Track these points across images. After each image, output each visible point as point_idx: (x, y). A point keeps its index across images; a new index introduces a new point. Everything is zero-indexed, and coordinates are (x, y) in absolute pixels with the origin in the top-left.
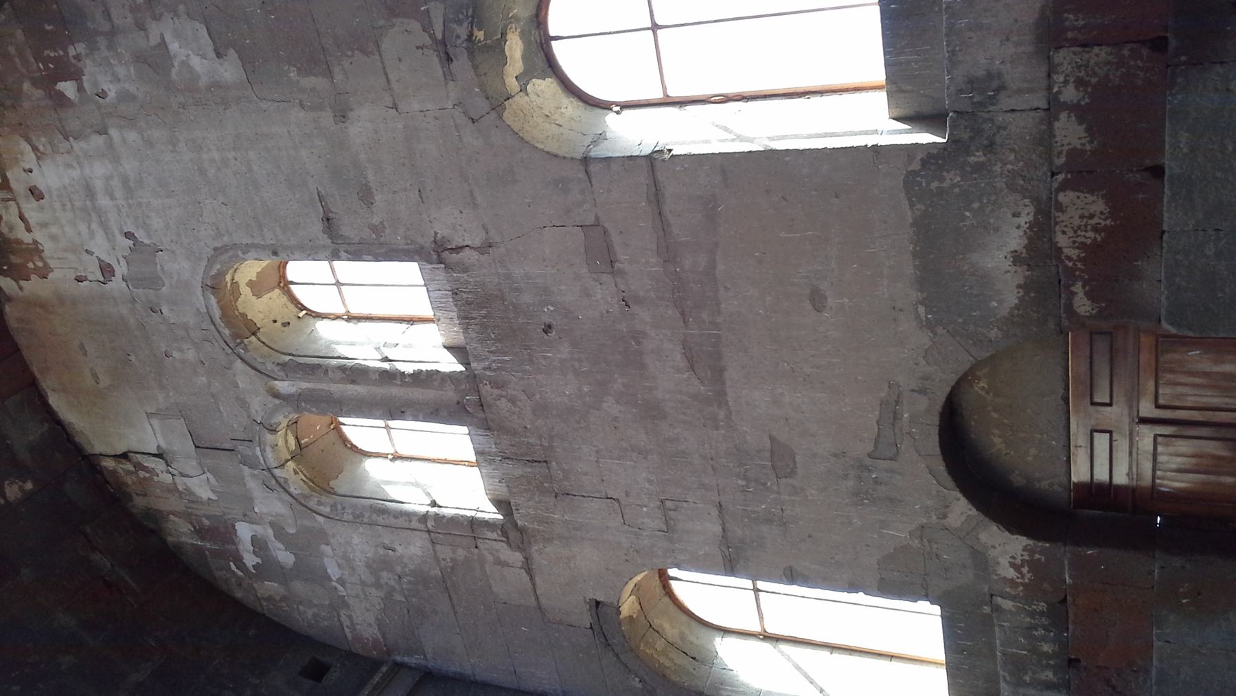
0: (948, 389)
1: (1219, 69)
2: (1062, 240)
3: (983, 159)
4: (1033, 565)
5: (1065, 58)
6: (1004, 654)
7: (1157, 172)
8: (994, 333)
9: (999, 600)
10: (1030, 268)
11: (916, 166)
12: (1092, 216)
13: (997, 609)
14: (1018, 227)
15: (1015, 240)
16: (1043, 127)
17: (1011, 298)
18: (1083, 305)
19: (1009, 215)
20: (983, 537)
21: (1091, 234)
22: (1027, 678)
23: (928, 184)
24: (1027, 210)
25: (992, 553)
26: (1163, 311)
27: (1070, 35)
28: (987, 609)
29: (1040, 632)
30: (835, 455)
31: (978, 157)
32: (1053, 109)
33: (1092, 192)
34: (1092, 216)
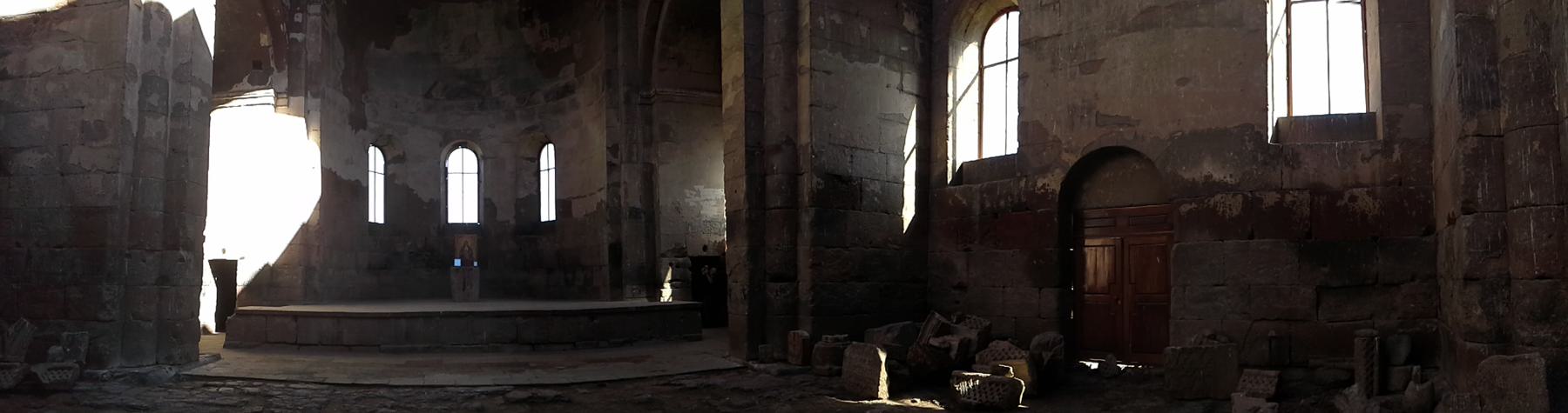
0: (1138, 149)
1: (1297, 260)
2: (1218, 197)
3: (1259, 160)
4: (1046, 194)
5: (1307, 195)
6: (996, 184)
7: (1251, 237)
8: (1169, 169)
9: (1025, 180)
10: (1203, 184)
11: (1257, 129)
12: (1230, 210)
13: (1020, 179)
14: (1225, 177)
15: (1218, 176)
16: (1274, 187)
17: (1187, 176)
18: (1185, 208)
19: (1231, 173)
20: (1058, 171)
21: (1221, 210)
22: (985, 195)
23: (1247, 135)
24: (1233, 180)
25: (1049, 175)
26: (1183, 243)
27: (1316, 198)
28: (1019, 174)
29: (1010, 199)
30: (1096, 95)
31: (1260, 158)
32: (1282, 191)
33: (1242, 209)
34: (1230, 210)
